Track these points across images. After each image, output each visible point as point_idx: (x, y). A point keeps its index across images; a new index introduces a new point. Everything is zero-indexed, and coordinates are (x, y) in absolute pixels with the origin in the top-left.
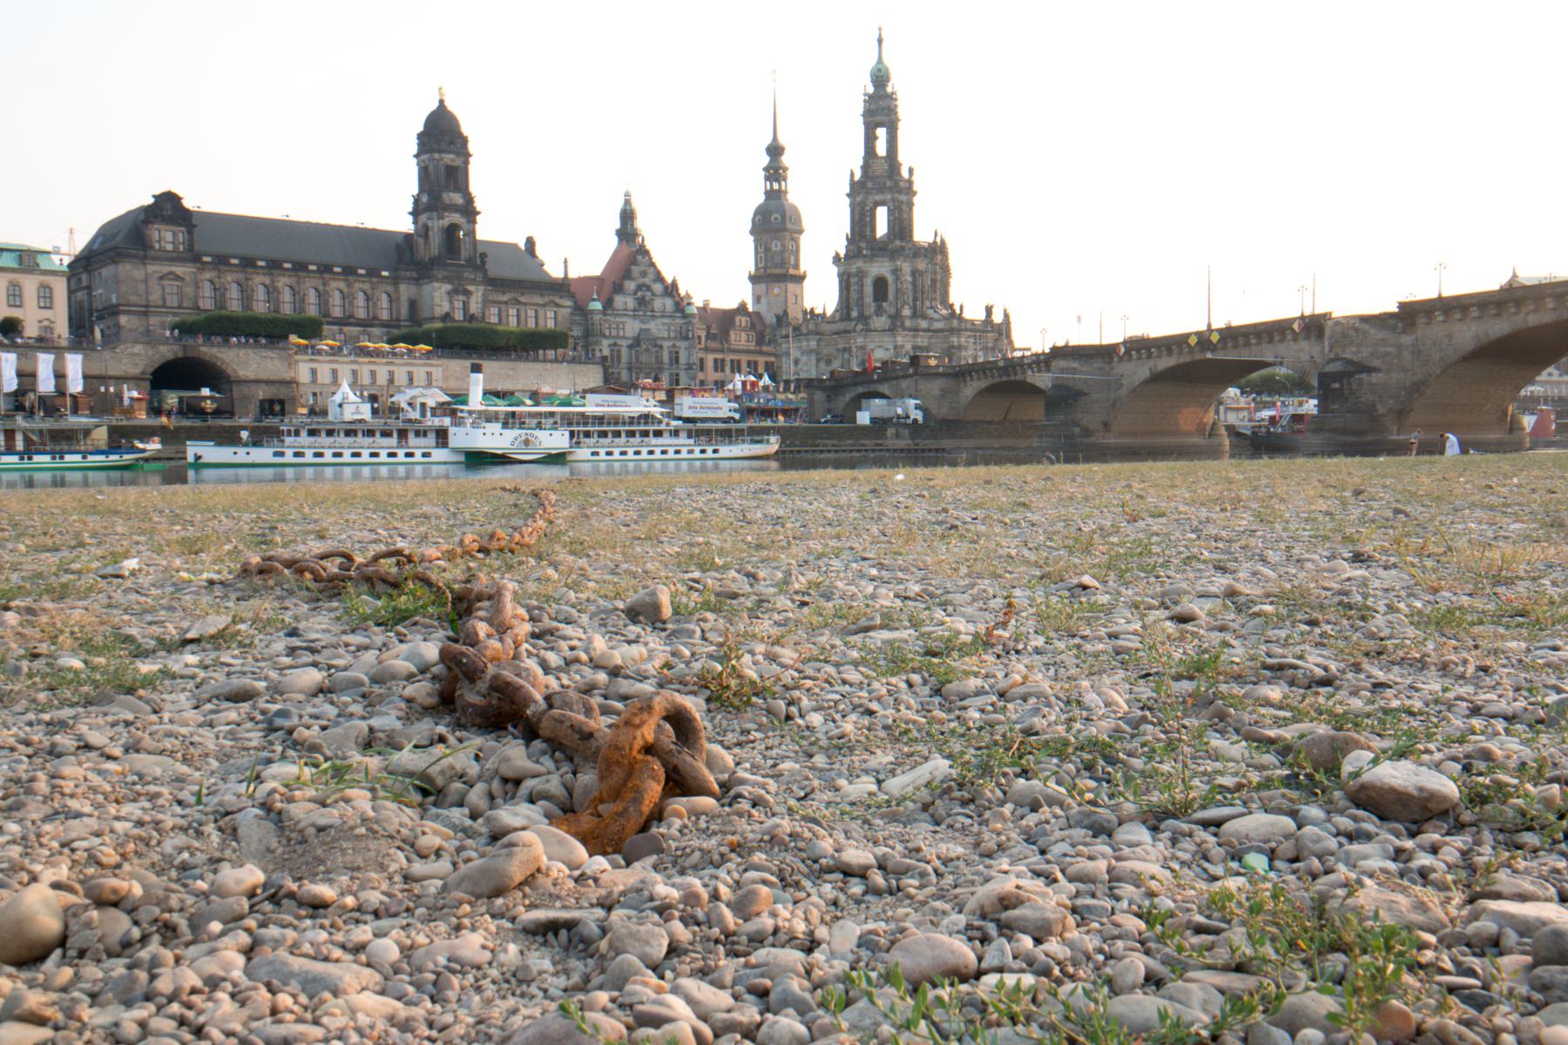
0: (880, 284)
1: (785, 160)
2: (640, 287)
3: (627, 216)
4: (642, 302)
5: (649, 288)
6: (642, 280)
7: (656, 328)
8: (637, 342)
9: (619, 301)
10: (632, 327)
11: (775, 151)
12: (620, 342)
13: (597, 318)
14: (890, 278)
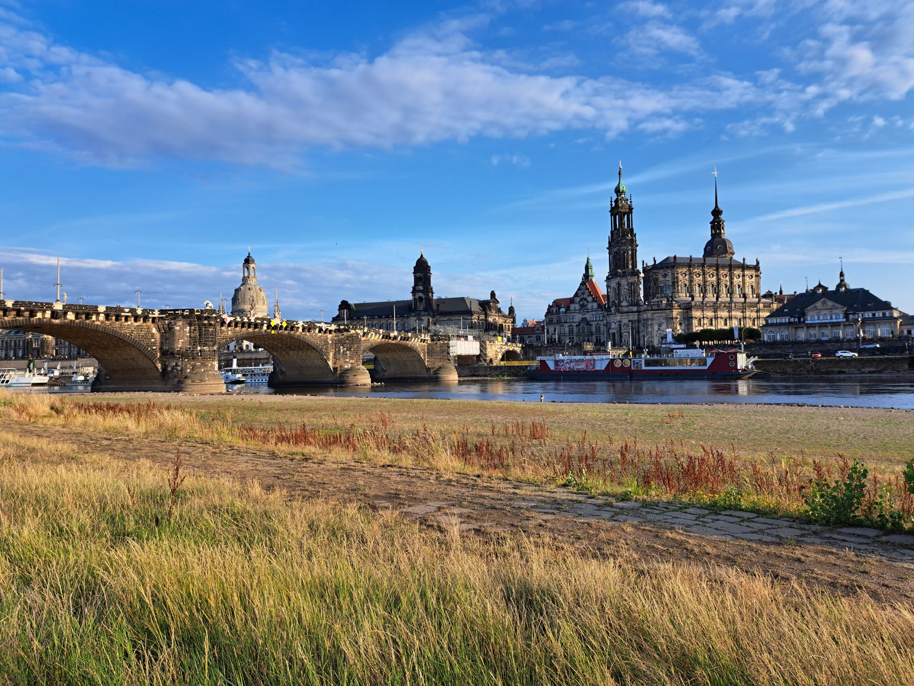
1: (722, 217)
2: (581, 300)
3: (587, 268)
4: (582, 306)
5: (586, 299)
7: (588, 316)
9: (572, 306)
10: (578, 317)
11: (716, 213)
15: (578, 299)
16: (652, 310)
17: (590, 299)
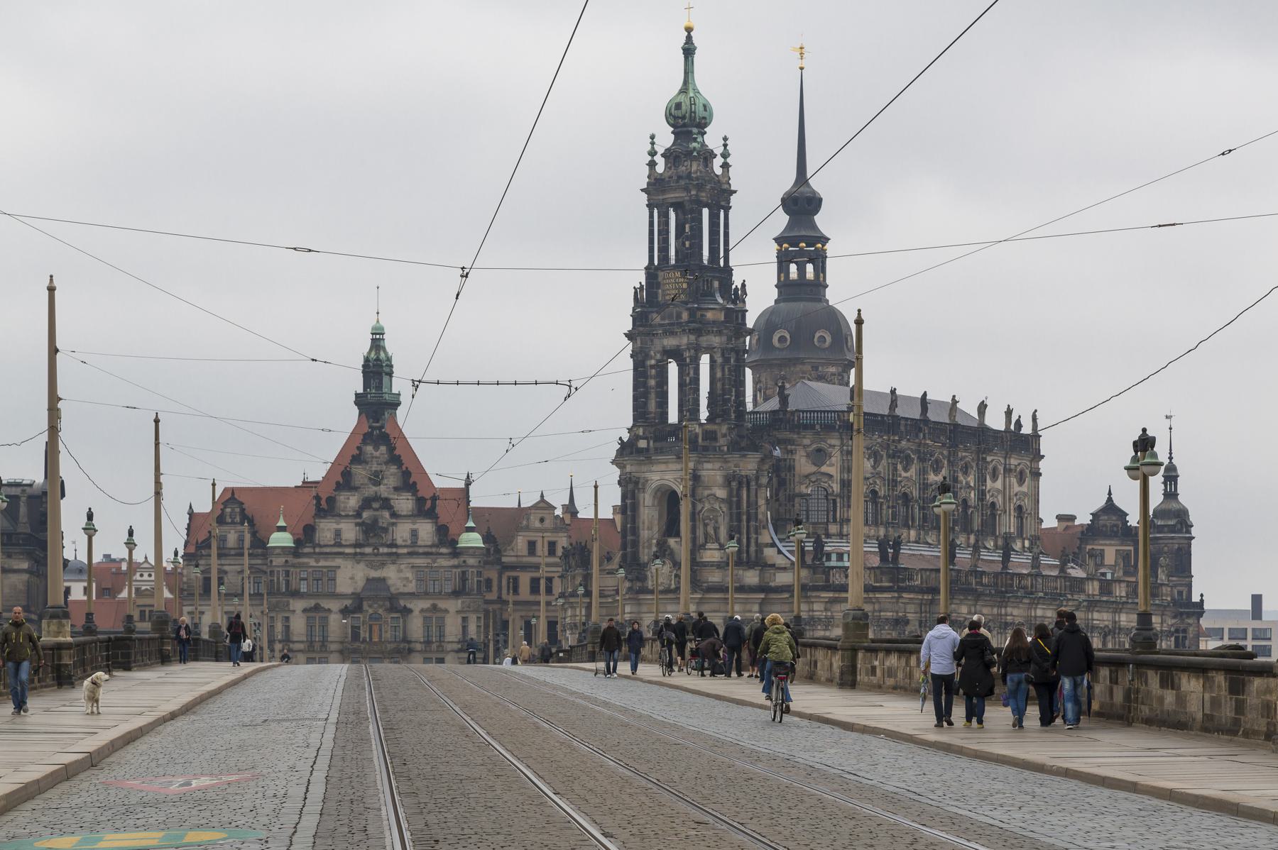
0: (670, 500)
2: (366, 503)
3: (376, 369)
4: (371, 531)
5: (386, 504)
6: (371, 490)
7: (398, 577)
8: (355, 606)
9: (326, 530)
10: (351, 577)
12: (326, 604)
13: (278, 561)
14: (679, 489)
15: (351, 501)
16: (827, 588)
17: (404, 503)
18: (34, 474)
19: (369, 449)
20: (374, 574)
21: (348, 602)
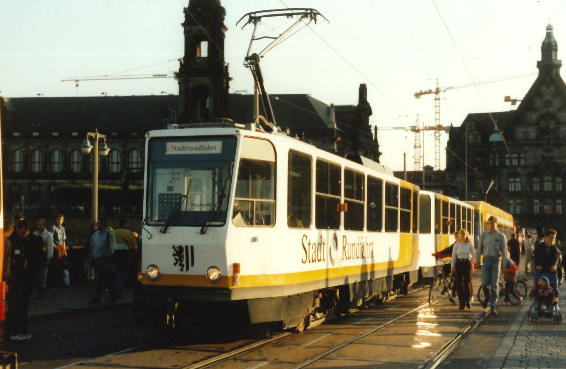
2: (542, 117)
3: (549, 47)
5: (553, 117)
6: (544, 111)
9: (520, 132)
15: (534, 117)
18: (354, 101)
19: (544, 88)
20: (546, 155)
21: (531, 170)
